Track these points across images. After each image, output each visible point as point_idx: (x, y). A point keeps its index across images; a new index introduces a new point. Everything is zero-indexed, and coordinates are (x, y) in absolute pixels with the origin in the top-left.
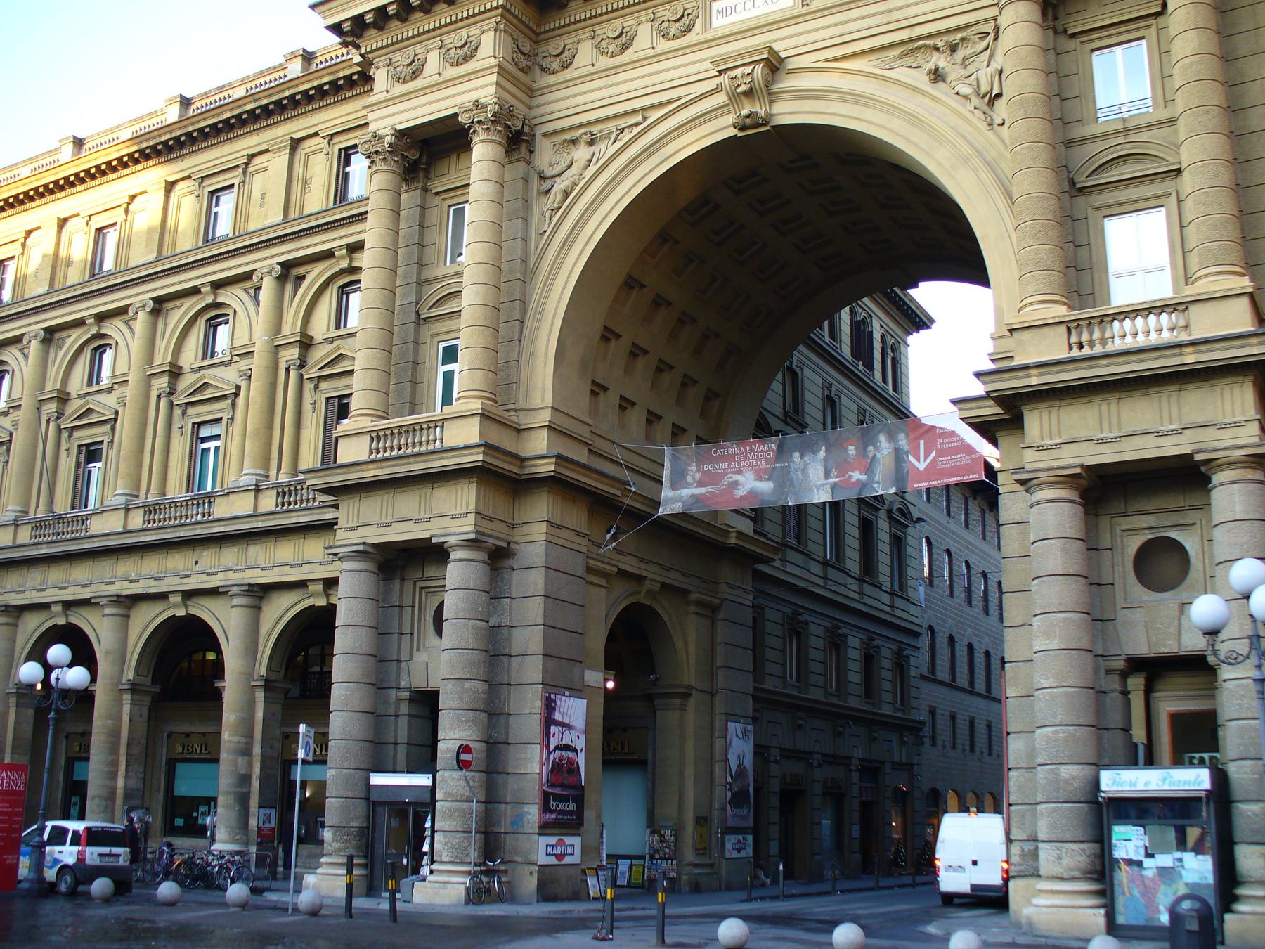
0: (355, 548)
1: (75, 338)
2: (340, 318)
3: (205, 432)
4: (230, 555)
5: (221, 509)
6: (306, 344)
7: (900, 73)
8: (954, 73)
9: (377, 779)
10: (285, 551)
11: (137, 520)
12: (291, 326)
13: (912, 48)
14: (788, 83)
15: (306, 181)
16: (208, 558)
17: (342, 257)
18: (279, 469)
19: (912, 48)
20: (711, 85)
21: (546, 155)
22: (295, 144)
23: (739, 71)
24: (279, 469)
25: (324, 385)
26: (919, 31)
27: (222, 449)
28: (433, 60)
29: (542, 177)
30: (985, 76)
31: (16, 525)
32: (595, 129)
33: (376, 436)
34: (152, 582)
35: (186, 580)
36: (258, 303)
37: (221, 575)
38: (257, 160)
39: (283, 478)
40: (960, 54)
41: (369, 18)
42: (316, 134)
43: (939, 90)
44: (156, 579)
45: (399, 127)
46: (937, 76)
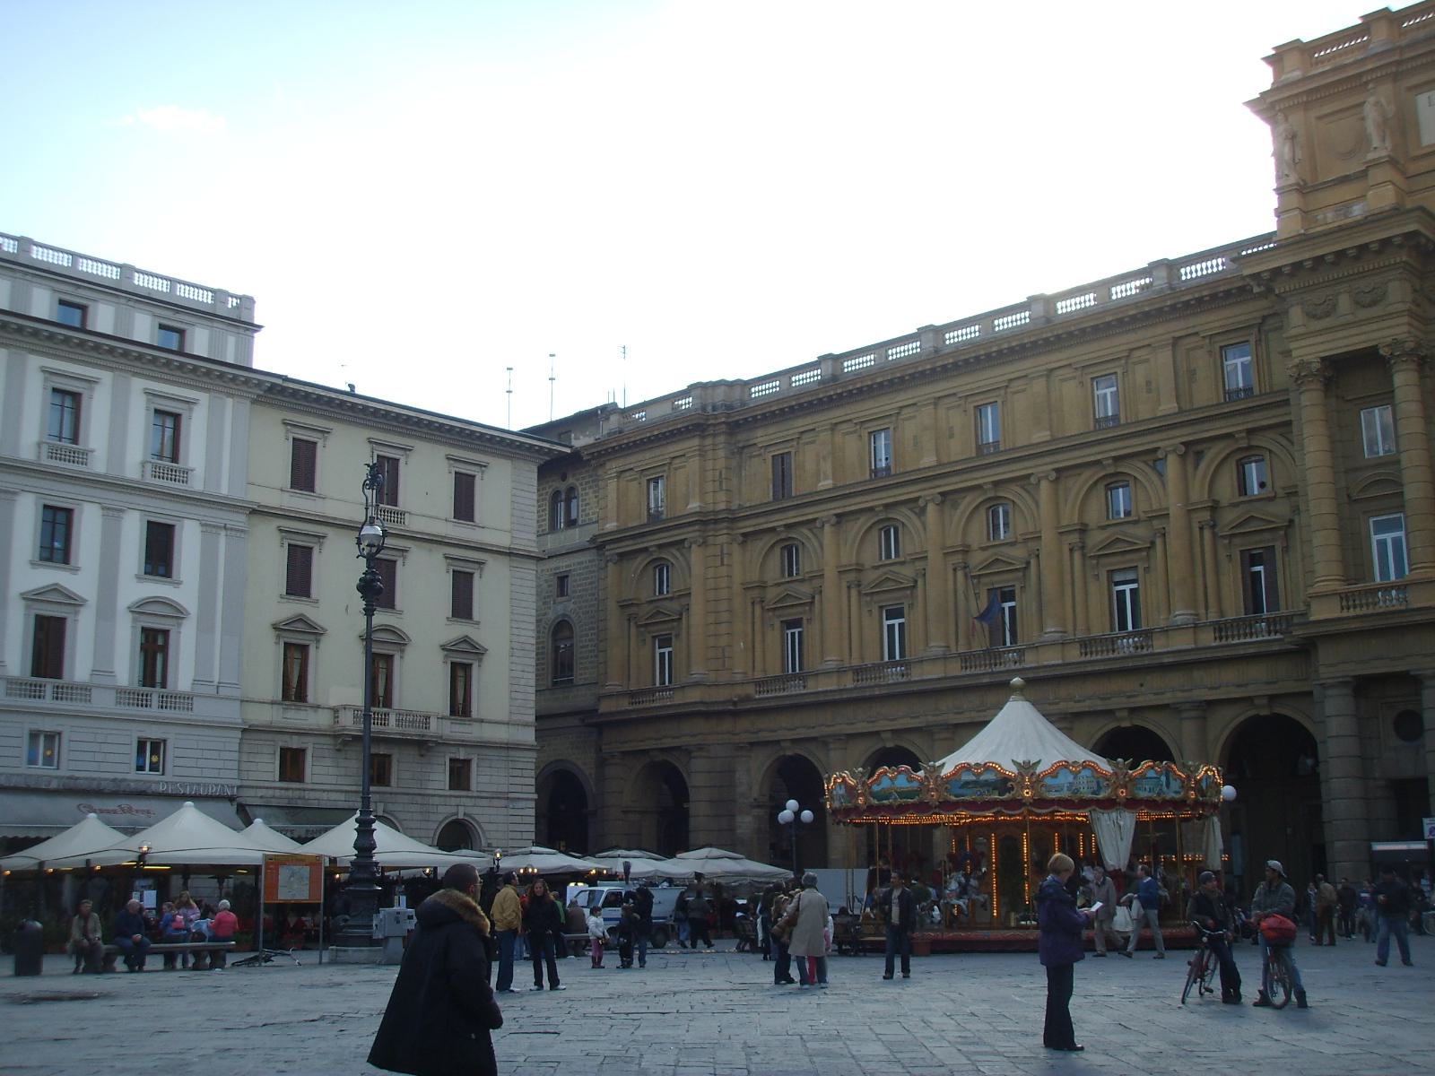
0: (1341, 680)
1: (969, 501)
2: (1243, 487)
3: (1117, 578)
4: (1176, 679)
5: (1159, 645)
6: (1215, 507)
9: (1379, 847)
10: (1229, 675)
11: (1074, 654)
12: (1198, 493)
15: (1192, 373)
16: (1155, 682)
17: (1242, 438)
18: (1207, 608)
22: (1176, 341)
24: (1207, 608)
25: (1237, 541)
27: (1141, 592)
28: (1344, 303)
31: (945, 658)
33: (1344, 596)
34: (1099, 702)
35: (1132, 700)
36: (1161, 475)
37: (1168, 695)
38: (1137, 354)
39: (1213, 617)
41: (1286, 270)
42: (1197, 334)
44: (1102, 699)
45: (1323, 355)
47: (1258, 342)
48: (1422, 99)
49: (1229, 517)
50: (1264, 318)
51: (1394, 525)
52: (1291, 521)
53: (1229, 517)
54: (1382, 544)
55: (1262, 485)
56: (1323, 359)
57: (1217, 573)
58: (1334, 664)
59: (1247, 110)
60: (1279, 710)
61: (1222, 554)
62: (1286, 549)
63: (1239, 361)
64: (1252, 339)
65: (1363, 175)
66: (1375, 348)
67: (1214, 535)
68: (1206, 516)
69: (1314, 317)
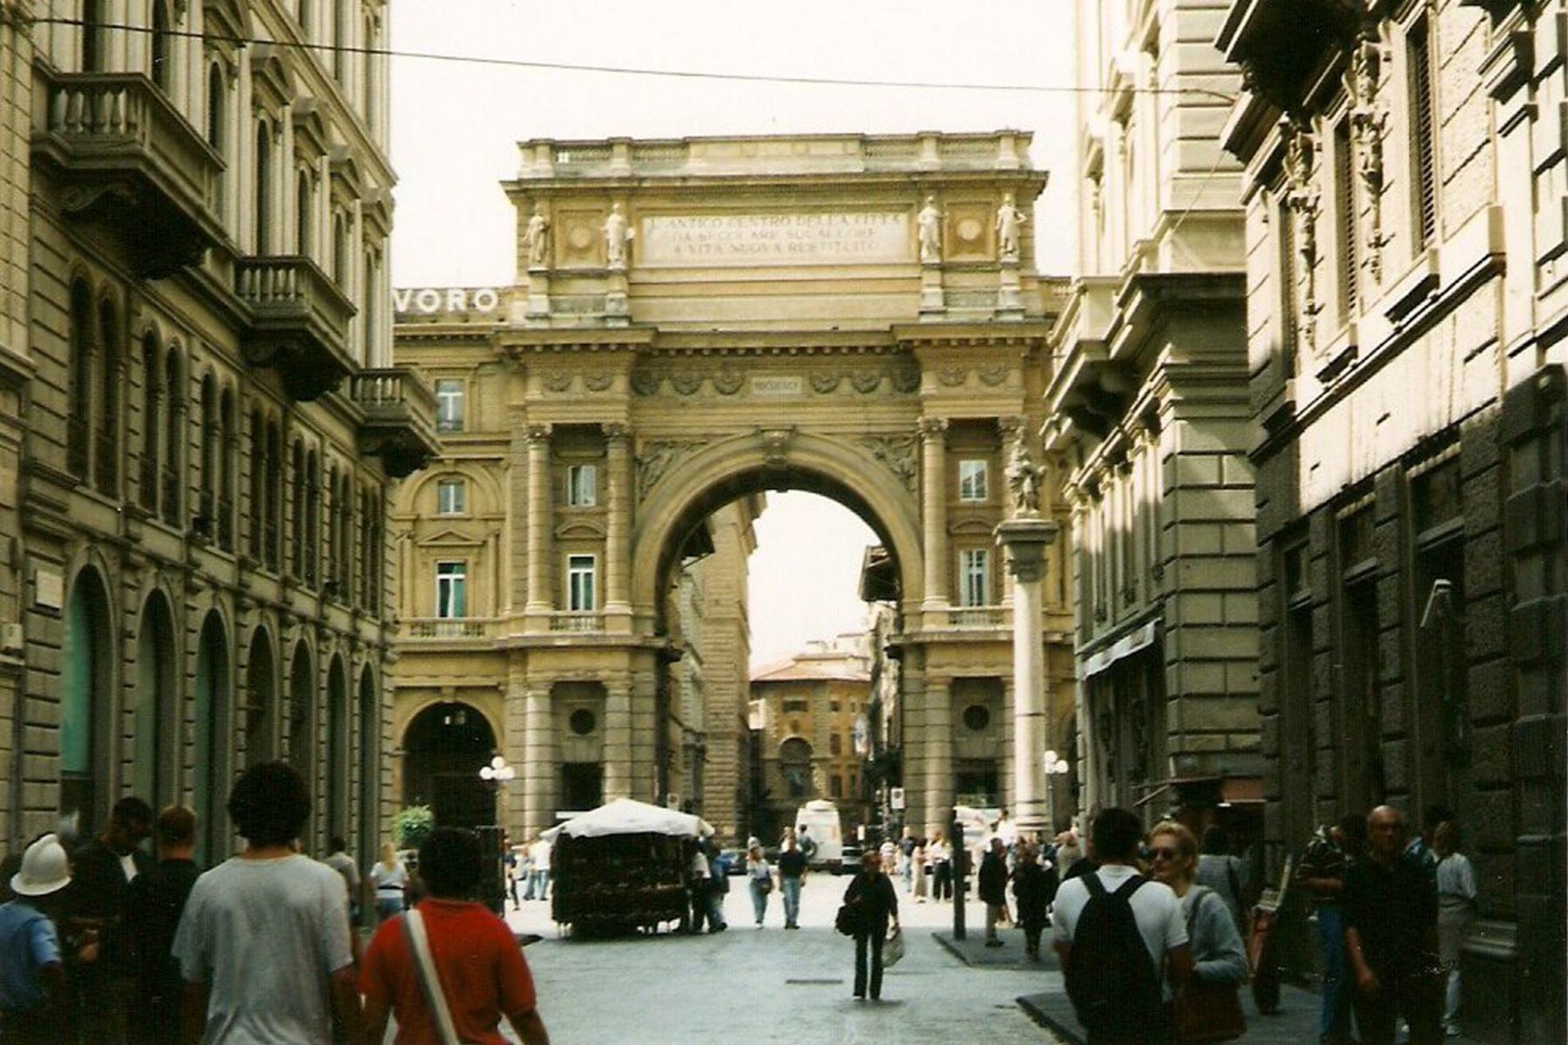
2: (442, 505)
6: (416, 521)
7: (861, 450)
8: (890, 456)
13: (869, 438)
14: (800, 442)
19: (869, 438)
20: (751, 431)
21: (639, 448)
23: (776, 434)
26: (873, 429)
28: (578, 385)
29: (641, 464)
30: (907, 461)
32: (678, 439)
40: (894, 445)
43: (880, 464)
46: (881, 457)
47: (472, 383)
48: (647, 222)
49: (429, 531)
50: (482, 364)
51: (589, 561)
52: (485, 543)
53: (429, 531)
54: (575, 576)
55: (458, 508)
56: (555, 426)
57: (414, 576)
58: (542, 669)
59: (501, 191)
60: (462, 699)
61: (419, 561)
62: (477, 564)
63: (451, 395)
64: (468, 379)
65: (603, 275)
66: (599, 425)
67: (414, 544)
68: (408, 526)
69: (551, 389)
